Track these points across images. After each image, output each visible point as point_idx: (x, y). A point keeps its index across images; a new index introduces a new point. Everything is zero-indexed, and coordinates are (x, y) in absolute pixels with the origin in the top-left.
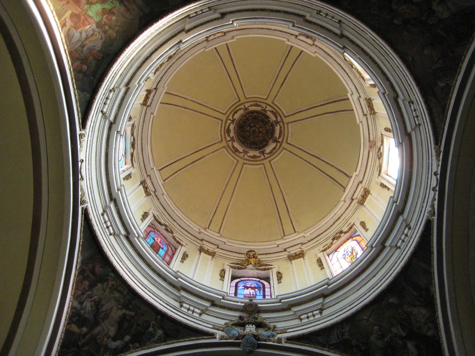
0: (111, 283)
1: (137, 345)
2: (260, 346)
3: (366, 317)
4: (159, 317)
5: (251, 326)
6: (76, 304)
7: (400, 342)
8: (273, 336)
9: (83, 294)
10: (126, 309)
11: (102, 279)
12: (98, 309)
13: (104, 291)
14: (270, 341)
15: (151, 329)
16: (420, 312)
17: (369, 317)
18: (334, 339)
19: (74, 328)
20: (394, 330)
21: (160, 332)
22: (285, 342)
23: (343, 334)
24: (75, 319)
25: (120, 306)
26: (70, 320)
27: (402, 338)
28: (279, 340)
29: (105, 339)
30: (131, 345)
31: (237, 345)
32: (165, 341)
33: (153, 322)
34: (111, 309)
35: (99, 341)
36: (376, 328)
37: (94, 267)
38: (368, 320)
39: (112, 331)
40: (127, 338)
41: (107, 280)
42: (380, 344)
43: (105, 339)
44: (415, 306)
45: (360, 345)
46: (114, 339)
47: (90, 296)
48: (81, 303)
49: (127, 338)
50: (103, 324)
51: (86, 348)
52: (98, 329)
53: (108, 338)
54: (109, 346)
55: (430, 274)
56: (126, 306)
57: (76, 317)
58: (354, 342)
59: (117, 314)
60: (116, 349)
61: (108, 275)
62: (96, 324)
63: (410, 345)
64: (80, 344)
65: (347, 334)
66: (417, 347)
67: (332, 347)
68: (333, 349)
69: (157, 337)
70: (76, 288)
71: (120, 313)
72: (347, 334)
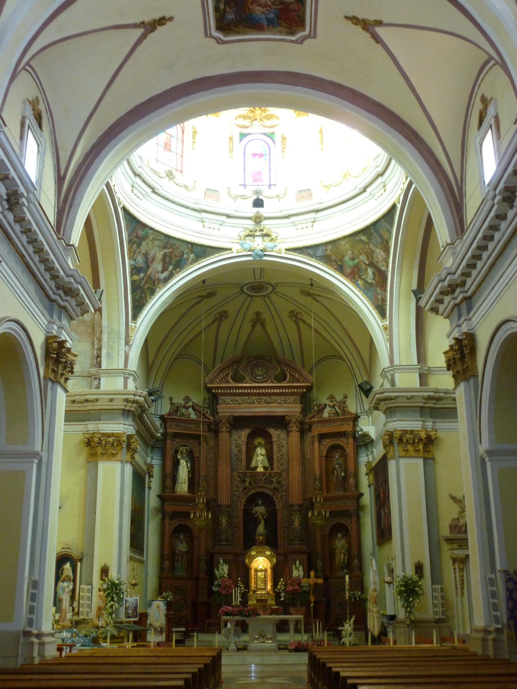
0: (151, 238)
1: (178, 270)
2: (265, 255)
3: (344, 243)
4: (190, 245)
5: (258, 237)
6: (132, 262)
7: (364, 266)
8: (275, 246)
9: (134, 254)
10: (165, 249)
11: (144, 238)
12: (146, 258)
13: (148, 244)
14: (273, 251)
15: (185, 256)
16: (379, 253)
17: (346, 243)
18: (320, 252)
19: (136, 277)
20: (362, 257)
21: (192, 256)
22: (285, 253)
23: (326, 250)
24: (134, 272)
25: (160, 249)
26: (132, 274)
27: (365, 264)
28: (280, 252)
29: (157, 274)
30: (174, 272)
31: (250, 255)
32: (196, 261)
33: (186, 251)
34: (155, 254)
35: (153, 278)
36: (350, 252)
37: (137, 234)
38: (345, 245)
39: (160, 267)
40: (171, 268)
41: (148, 237)
42: (351, 263)
43: (157, 274)
44: (378, 248)
45: (338, 260)
46: (162, 272)
47: (140, 253)
48: (135, 260)
49: (171, 268)
50: (152, 266)
51: (146, 286)
52: (151, 269)
53: (158, 273)
54: (160, 278)
55: (390, 233)
56: (165, 247)
57: (135, 270)
58: (333, 258)
59: (160, 255)
60: (165, 279)
61: (147, 233)
62: (148, 267)
63: (370, 271)
64: (142, 285)
65: (329, 250)
66: (374, 274)
67: (318, 258)
68: (318, 260)
69: (190, 260)
70: (129, 252)
71: (162, 253)
72: (329, 250)
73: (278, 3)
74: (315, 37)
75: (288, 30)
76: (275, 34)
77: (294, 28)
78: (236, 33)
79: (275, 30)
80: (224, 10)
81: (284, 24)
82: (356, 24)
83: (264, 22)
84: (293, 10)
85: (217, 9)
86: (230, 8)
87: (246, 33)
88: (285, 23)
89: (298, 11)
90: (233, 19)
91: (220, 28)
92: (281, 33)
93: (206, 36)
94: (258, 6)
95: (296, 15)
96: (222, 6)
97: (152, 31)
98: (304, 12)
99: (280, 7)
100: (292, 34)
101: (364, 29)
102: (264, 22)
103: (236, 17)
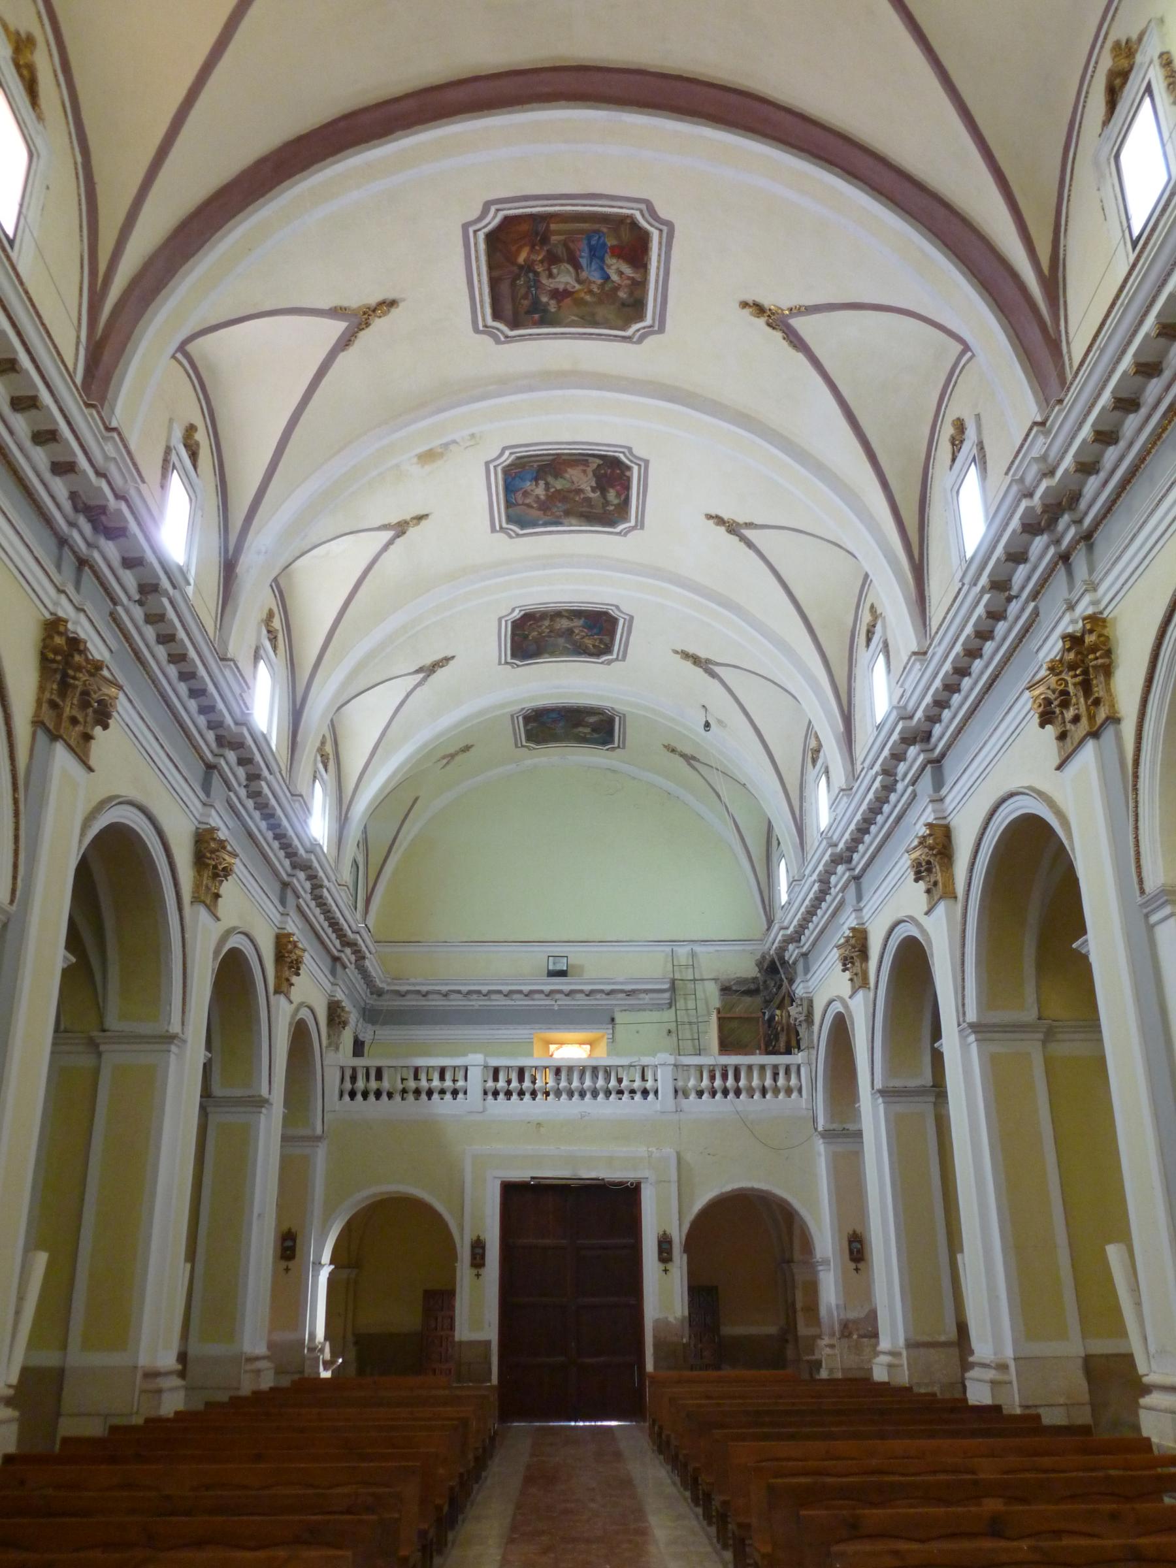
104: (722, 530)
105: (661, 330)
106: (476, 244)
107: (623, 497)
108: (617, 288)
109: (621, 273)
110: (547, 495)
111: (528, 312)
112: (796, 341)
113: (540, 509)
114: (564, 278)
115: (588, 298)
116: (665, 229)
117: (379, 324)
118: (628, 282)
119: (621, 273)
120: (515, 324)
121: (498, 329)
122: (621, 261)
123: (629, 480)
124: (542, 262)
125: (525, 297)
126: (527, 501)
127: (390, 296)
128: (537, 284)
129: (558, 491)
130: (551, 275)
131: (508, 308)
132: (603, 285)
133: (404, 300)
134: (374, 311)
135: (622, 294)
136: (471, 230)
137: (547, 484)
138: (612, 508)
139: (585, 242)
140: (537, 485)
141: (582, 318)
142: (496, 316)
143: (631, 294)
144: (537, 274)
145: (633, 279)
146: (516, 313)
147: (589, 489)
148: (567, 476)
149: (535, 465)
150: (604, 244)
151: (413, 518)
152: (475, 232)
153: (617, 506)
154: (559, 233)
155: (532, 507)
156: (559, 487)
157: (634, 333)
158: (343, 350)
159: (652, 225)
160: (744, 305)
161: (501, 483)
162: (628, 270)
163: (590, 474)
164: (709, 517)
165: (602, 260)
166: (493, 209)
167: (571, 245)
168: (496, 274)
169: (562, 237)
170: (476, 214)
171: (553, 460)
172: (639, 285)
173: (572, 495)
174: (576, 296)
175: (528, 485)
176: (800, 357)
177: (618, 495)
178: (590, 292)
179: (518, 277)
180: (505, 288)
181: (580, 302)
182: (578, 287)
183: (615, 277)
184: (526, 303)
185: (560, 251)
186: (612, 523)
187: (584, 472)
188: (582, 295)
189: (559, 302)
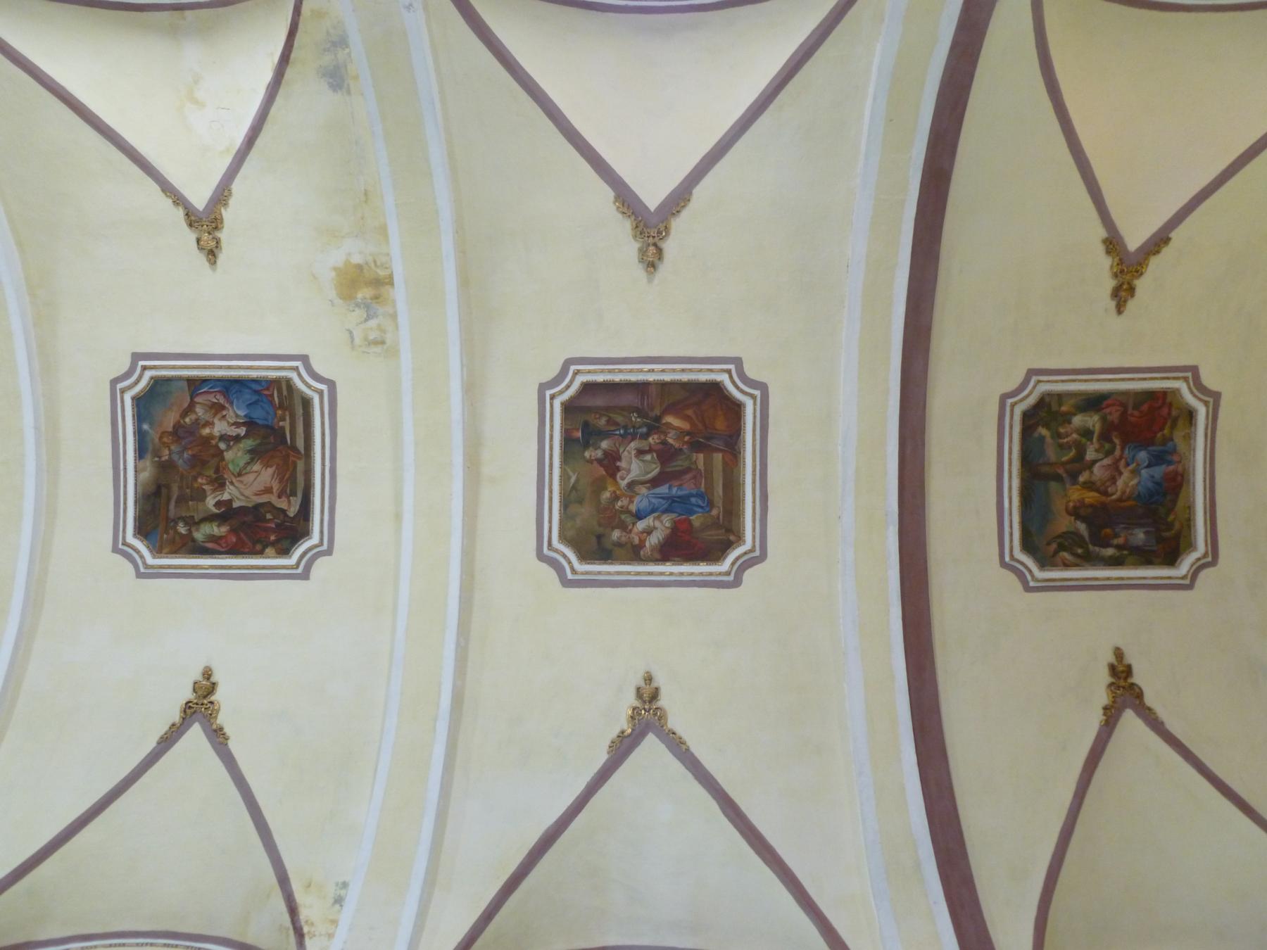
73: (1107, 446)
74: (1194, 370)
75: (1180, 423)
76: (1192, 450)
77: (1174, 413)
78: (1189, 527)
79: (1181, 447)
80: (1118, 547)
81: (1166, 431)
82: (1132, 290)
83: (1158, 471)
84: (1124, 414)
85: (1116, 562)
86: (1116, 536)
87: (1190, 508)
88: (1162, 429)
89: (1124, 406)
90: (1146, 533)
91: (1171, 558)
92: (1190, 437)
93: (1190, 587)
94: (1114, 483)
95: (1136, 407)
96: (1110, 552)
97: (1140, 695)
98: (1126, 393)
99: (1117, 441)
100: (1191, 415)
101: (1139, 273)
102: (1158, 471)
103: (1141, 526)
104: (187, 694)
105: (566, 583)
106: (711, 371)
107: (210, 545)
108: (623, 527)
109: (649, 532)
110: (211, 437)
111: (586, 425)
112: (622, 748)
113: (178, 426)
114: (634, 467)
115: (606, 495)
116: (731, 578)
117: (630, 248)
118: (636, 541)
119: (649, 532)
120: (569, 409)
121: (568, 387)
122: (668, 531)
123: (260, 553)
124: (664, 443)
125: (610, 421)
126: (199, 410)
127: (665, 268)
128: (629, 436)
129: (220, 454)
130: (640, 453)
131: (599, 401)
132: (628, 512)
133: (650, 281)
134: (655, 245)
135: (616, 534)
136: (732, 367)
137: (237, 439)
138: (182, 529)
139: (694, 492)
140: (237, 425)
141: (574, 487)
142: (588, 388)
143: (619, 545)
144: (645, 437)
145: (642, 544)
146: (589, 410)
147: (226, 497)
148: (257, 467)
149: (286, 424)
150: (692, 512)
151: (218, 242)
152: (729, 372)
153: (189, 538)
154: (709, 463)
155: (185, 413)
156: (228, 455)
157: (556, 551)
158: (617, 198)
159: (733, 564)
160: (649, 679)
161: (254, 374)
162: (654, 540)
163: (264, 499)
164: (207, 674)
165: (666, 511)
166: (757, 393)
167: (688, 476)
168: (653, 391)
169: (701, 465)
170: (751, 373)
171: (294, 448)
172: (635, 554)
173: (211, 472)
174: (609, 480)
175: (238, 411)
176: (601, 757)
177: (213, 538)
178: (616, 498)
179: (641, 413)
180: (629, 399)
181: (599, 486)
182: (623, 483)
183: (641, 525)
184: (603, 421)
185: (679, 464)
186: (142, 530)
187: (268, 490)
188: (611, 488)
189: (599, 461)
